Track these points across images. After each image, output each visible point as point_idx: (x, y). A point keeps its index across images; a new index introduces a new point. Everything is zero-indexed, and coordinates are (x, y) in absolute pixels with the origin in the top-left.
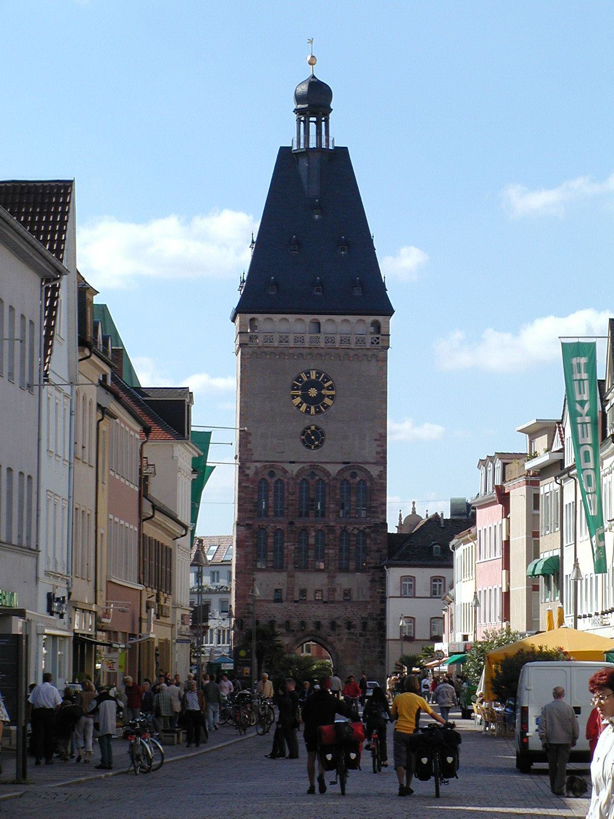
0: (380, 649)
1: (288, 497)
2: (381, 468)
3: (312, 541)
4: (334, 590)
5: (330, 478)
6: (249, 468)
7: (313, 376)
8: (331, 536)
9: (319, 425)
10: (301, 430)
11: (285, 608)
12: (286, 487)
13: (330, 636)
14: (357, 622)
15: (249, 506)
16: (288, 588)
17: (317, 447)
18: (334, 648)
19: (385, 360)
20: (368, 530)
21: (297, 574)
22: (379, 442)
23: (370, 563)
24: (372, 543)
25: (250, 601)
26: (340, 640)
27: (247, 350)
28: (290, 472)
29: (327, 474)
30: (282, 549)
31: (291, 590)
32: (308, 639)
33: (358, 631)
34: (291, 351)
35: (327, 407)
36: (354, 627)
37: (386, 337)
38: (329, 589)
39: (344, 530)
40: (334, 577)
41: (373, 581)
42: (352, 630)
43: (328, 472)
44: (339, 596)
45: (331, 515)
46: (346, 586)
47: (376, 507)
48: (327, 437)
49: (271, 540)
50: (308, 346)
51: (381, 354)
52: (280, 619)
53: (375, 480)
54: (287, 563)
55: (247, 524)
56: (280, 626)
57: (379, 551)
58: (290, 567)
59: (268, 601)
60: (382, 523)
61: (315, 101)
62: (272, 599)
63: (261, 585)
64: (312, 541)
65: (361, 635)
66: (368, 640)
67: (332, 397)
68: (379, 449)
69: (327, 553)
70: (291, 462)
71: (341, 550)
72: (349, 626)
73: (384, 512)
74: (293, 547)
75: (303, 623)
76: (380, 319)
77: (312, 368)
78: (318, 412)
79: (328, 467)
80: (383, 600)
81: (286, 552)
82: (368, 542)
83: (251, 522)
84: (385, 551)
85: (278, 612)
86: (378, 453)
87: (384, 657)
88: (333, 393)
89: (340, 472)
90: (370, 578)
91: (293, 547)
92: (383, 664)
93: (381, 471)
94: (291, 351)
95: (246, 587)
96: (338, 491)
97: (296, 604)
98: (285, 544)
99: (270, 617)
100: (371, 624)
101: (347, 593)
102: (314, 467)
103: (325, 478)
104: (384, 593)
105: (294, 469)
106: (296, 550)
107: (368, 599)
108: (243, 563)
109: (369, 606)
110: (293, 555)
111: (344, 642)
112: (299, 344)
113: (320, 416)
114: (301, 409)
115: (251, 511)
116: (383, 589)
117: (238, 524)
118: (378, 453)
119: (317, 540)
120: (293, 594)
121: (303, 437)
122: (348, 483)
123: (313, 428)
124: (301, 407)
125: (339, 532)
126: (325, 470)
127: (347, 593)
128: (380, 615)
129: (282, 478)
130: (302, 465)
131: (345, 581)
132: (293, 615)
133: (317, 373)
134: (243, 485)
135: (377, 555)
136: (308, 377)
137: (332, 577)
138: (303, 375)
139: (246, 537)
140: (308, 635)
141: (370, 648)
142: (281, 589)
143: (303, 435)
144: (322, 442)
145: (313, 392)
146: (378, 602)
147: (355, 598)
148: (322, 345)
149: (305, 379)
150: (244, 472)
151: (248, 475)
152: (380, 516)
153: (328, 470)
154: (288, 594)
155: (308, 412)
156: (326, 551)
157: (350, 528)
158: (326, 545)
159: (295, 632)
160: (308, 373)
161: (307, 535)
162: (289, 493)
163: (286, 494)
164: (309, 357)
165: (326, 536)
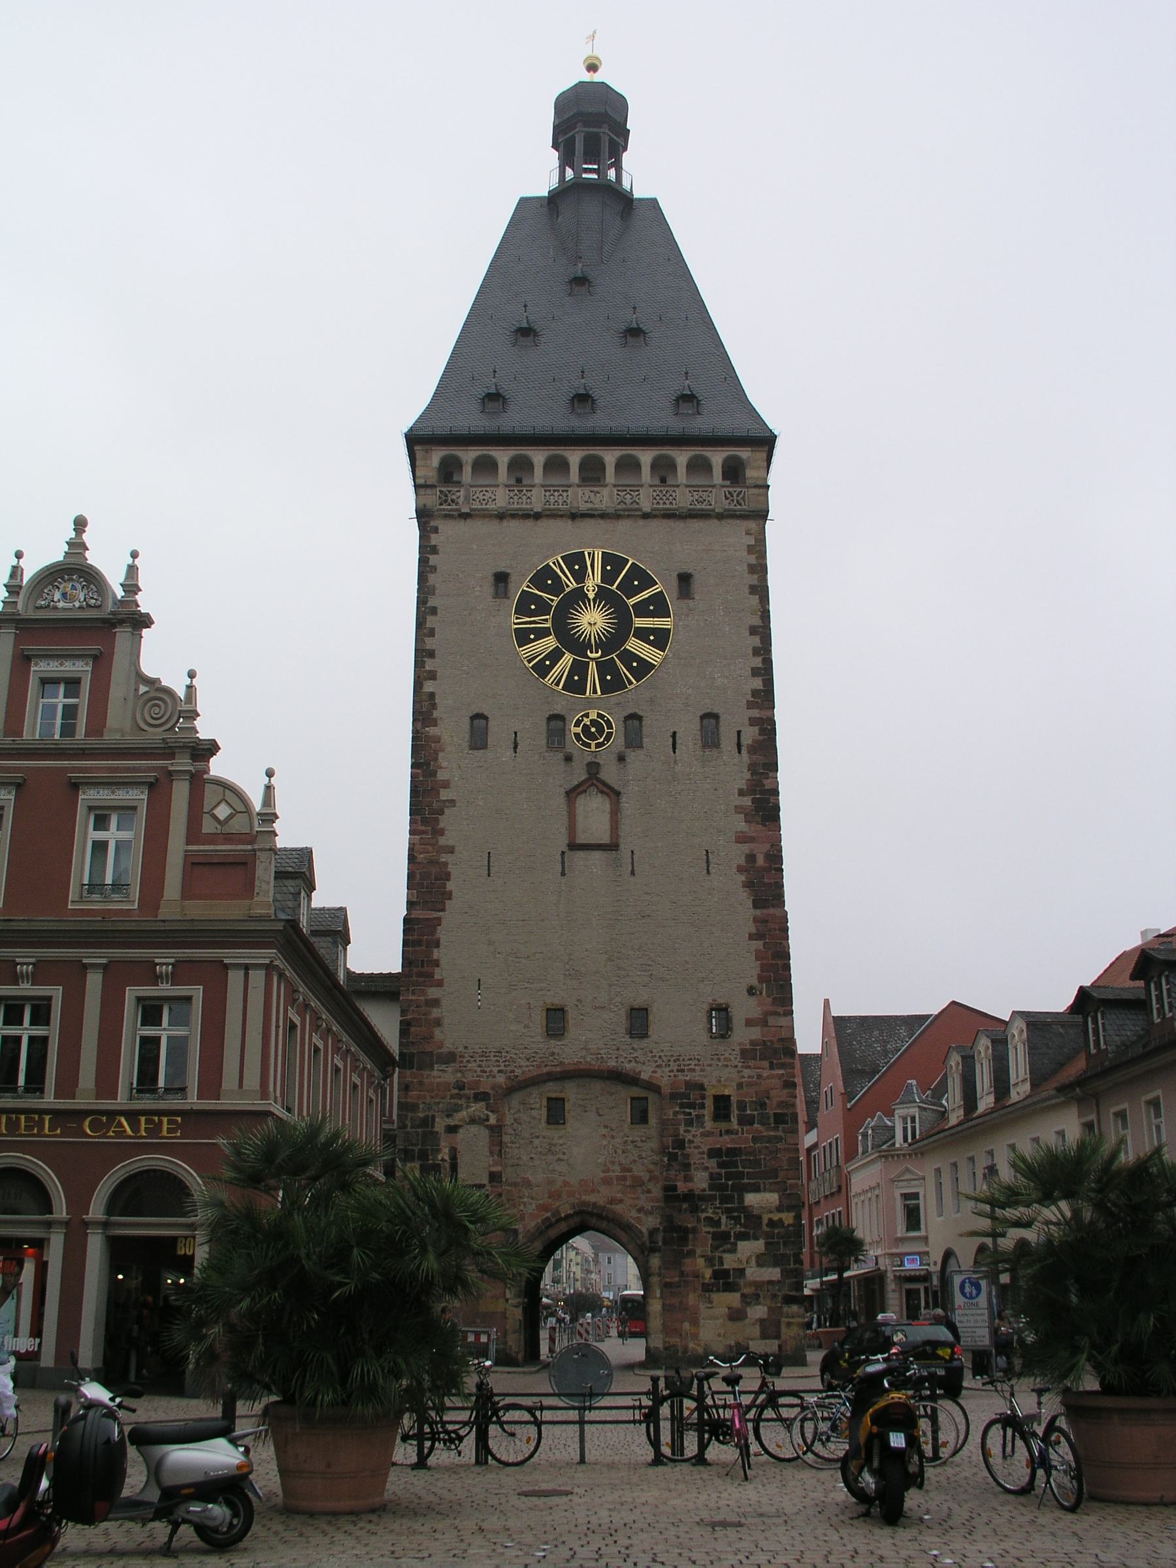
37: (761, 490)
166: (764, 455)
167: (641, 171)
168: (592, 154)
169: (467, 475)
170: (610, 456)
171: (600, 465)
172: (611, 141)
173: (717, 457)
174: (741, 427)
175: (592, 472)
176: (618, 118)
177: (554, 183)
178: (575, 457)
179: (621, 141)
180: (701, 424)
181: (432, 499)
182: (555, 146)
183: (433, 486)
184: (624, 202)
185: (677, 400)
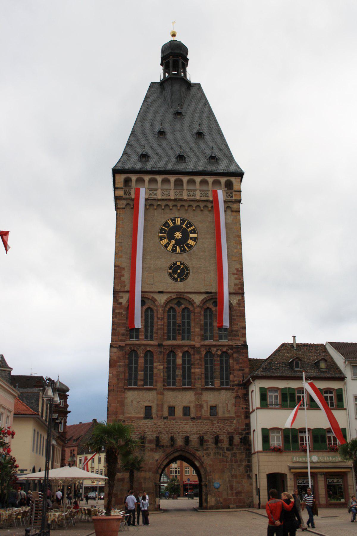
0: (247, 463)
1: (157, 322)
2: (240, 297)
3: (179, 361)
4: (201, 406)
5: (195, 306)
6: (122, 297)
7: (178, 222)
8: (197, 357)
9: (184, 261)
10: (168, 265)
11: (155, 424)
12: (155, 314)
13: (198, 451)
14: (225, 438)
15: (122, 330)
16: (158, 405)
17: (182, 280)
18: (202, 463)
19: (239, 211)
20: (230, 351)
21: (166, 392)
22: (236, 276)
23: (234, 381)
24: (235, 363)
25: (121, 417)
26: (208, 455)
27: (122, 202)
28: (158, 300)
29: (191, 302)
30: (152, 369)
31: (160, 407)
32: (176, 454)
33: (225, 444)
34: (159, 203)
35: (190, 247)
36: (222, 441)
38: (197, 405)
39: (209, 352)
40: (201, 394)
41: (237, 397)
42: (219, 445)
43: (193, 300)
44: (205, 412)
45: (196, 338)
46: (212, 403)
47: (236, 331)
48: (191, 271)
49: (141, 361)
50: (173, 198)
51: (234, 206)
52: (150, 436)
53: (235, 308)
54: (156, 382)
55: (120, 346)
56: (150, 442)
57: (241, 369)
58: (160, 385)
59: (139, 418)
60: (242, 345)
61: (175, 56)
62: (142, 415)
63: (132, 402)
64: (179, 361)
65: (228, 449)
66: (234, 455)
67: (195, 239)
68: (237, 282)
69: (194, 373)
70: (160, 292)
71: (206, 369)
72: (217, 440)
73: (244, 335)
74: (162, 367)
75: (172, 439)
76: (233, 179)
77: (177, 216)
78: (183, 251)
79: (193, 297)
80: (247, 415)
81: (155, 371)
82: (231, 361)
83: (123, 344)
84: (247, 370)
85: (149, 428)
86: (236, 285)
87: (251, 471)
88: (195, 235)
89: (204, 302)
90: (234, 395)
91: (162, 367)
92: (249, 477)
93: (239, 300)
94: (159, 203)
95: (118, 405)
96: (202, 318)
97: (165, 420)
98: (155, 364)
99: (140, 433)
100: (237, 439)
101: (213, 409)
102: (180, 298)
103: (190, 307)
104: (248, 408)
105: (162, 299)
106: (165, 370)
107: (234, 415)
108: (115, 381)
109: (235, 422)
110: (162, 374)
111: (212, 456)
112: (166, 197)
113: (185, 255)
114: (168, 249)
115: (123, 335)
116: (246, 405)
117: (111, 346)
118: (236, 285)
119: (184, 361)
120: (162, 411)
121: (170, 271)
122: (210, 309)
123: (179, 264)
124: (168, 247)
125: (204, 353)
126: (190, 299)
127: (213, 409)
128: (245, 430)
129: (151, 306)
130: (169, 295)
131: (210, 398)
132: (163, 431)
133: (181, 220)
134: (117, 311)
135: (240, 373)
136: (174, 223)
137: (198, 395)
138: (170, 222)
139: (119, 358)
140: (178, 451)
141: (237, 462)
142: (151, 407)
143: (170, 269)
144: (187, 275)
145: (178, 235)
146: (243, 418)
147: (220, 414)
148: (185, 197)
149: (171, 225)
150: (117, 300)
151: (121, 303)
152: (241, 339)
153: (193, 298)
154: (157, 411)
155: (174, 251)
156: (192, 371)
157: (214, 350)
158: (192, 364)
159: (165, 447)
160: (173, 220)
161: (175, 356)
162: (158, 319)
163: (155, 320)
164: (174, 208)
165: (192, 357)
166: (240, 180)
167: (193, 74)
168: (176, 68)
169: (133, 184)
170: (185, 179)
171: (181, 181)
172: (182, 62)
173: (223, 180)
174: (232, 169)
175: (179, 183)
176: (185, 54)
177: (162, 78)
178: (172, 178)
179: (186, 63)
180: (217, 168)
181: (120, 193)
182: (162, 64)
183: (122, 188)
184: (189, 85)
185: (209, 158)
